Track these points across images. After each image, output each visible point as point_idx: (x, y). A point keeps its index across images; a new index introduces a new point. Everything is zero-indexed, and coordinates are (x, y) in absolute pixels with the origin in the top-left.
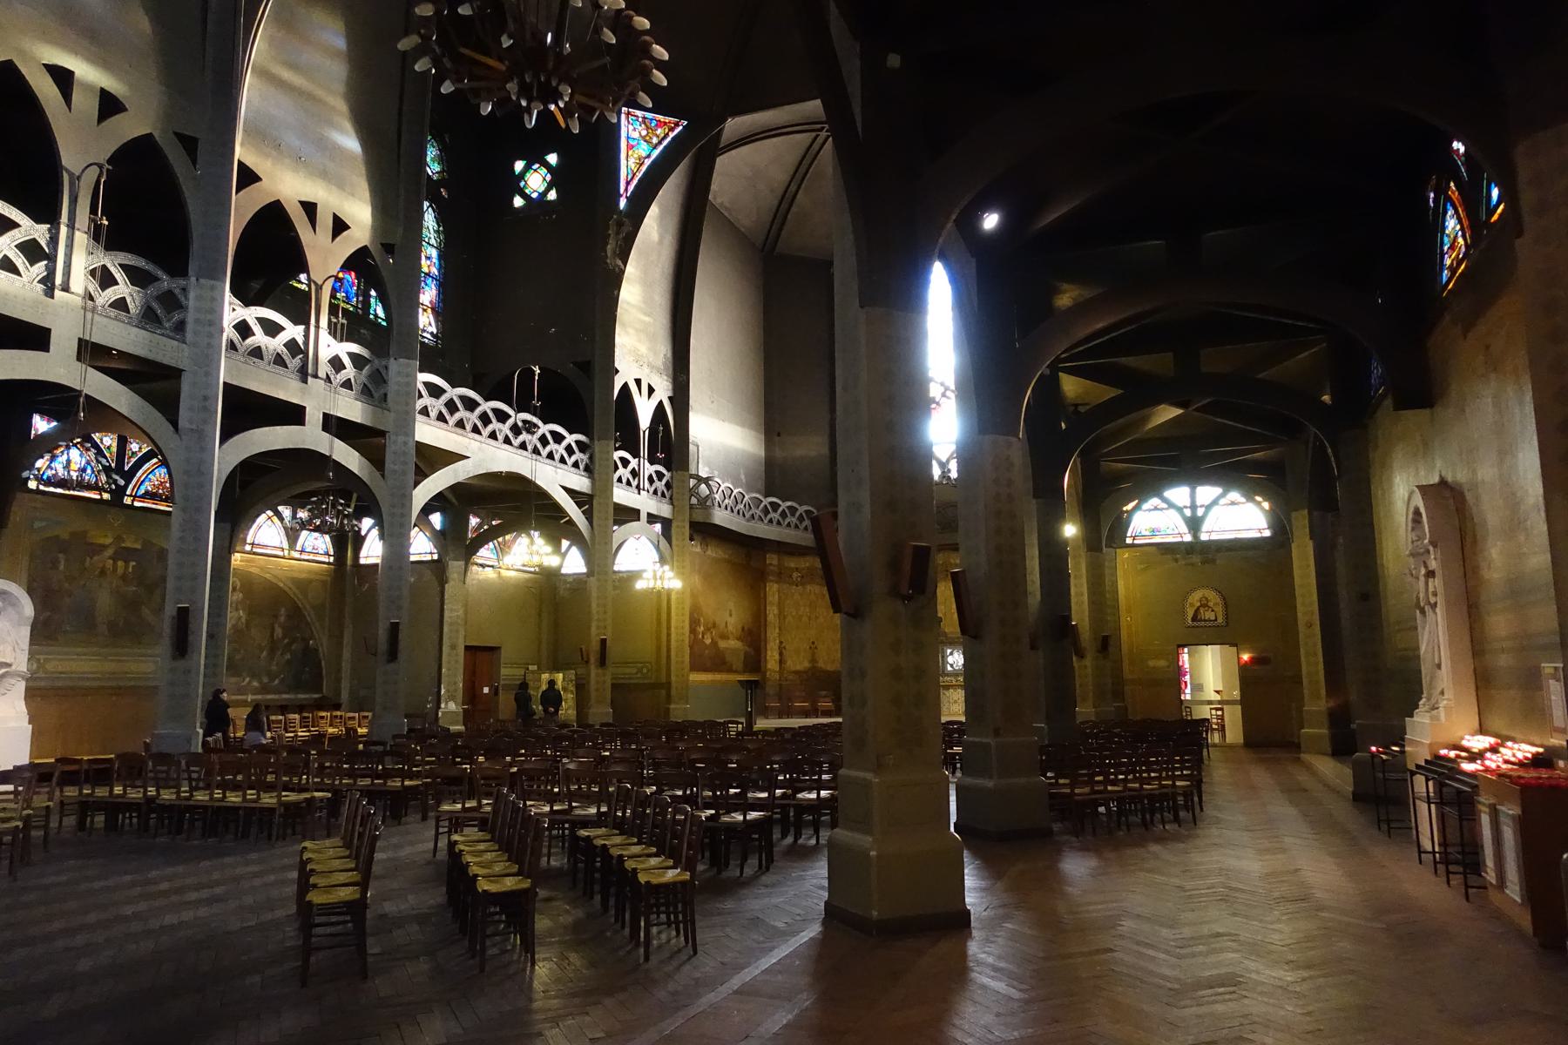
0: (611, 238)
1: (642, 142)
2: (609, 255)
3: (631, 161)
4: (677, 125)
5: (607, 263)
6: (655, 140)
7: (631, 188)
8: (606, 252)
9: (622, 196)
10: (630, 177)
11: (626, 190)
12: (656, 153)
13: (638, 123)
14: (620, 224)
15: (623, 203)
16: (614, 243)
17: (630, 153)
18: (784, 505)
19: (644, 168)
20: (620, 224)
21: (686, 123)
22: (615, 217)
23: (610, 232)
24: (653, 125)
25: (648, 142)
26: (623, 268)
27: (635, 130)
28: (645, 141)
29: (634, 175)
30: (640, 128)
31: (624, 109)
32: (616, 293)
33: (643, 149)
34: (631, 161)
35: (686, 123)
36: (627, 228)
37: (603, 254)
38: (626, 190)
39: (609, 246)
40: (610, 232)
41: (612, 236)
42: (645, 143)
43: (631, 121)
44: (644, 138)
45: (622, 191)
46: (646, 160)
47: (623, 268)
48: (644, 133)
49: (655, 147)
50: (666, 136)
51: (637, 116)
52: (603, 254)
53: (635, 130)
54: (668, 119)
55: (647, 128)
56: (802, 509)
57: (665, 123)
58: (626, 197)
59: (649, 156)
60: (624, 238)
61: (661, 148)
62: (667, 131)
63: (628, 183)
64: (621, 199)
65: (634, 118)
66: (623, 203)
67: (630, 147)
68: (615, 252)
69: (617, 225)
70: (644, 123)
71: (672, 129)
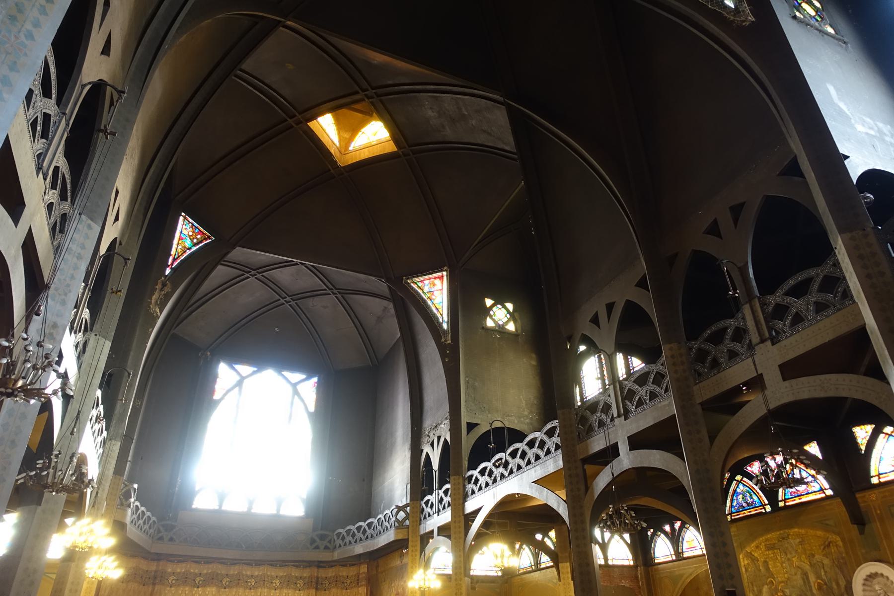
0: (157, 292)
1: (188, 238)
2: (153, 302)
3: (180, 247)
4: (209, 238)
5: (150, 307)
6: (195, 241)
7: (176, 264)
8: (151, 299)
9: (168, 266)
10: (176, 257)
11: (172, 264)
12: (194, 249)
13: (189, 226)
14: (164, 285)
15: (168, 271)
16: (158, 296)
17: (180, 242)
18: (148, 514)
19: (185, 255)
20: (164, 285)
21: (214, 239)
22: (163, 278)
23: (157, 287)
24: (196, 231)
25: (192, 241)
26: (159, 314)
27: (186, 229)
28: (190, 239)
29: (179, 257)
30: (189, 230)
31: (183, 214)
32: (150, 330)
33: (188, 243)
34: (180, 247)
35: (214, 239)
36: (167, 289)
37: (149, 300)
38: (172, 264)
39: (154, 296)
40: (157, 287)
41: (158, 290)
42: (190, 240)
43: (185, 223)
44: (190, 236)
45: (169, 263)
46: (188, 251)
47: (159, 314)
48: (191, 234)
49: (195, 245)
50: (201, 242)
51: (189, 221)
52: (149, 300)
53: (186, 229)
54: (205, 232)
55: (193, 232)
56: (153, 519)
57: (203, 233)
58: (172, 268)
59: (189, 249)
60: (164, 294)
61: (198, 247)
62: (203, 238)
63: (174, 260)
64: (168, 269)
65: (187, 222)
66: (168, 271)
67: (181, 238)
68: (157, 302)
69: (162, 285)
70: (192, 228)
71: (206, 239)
